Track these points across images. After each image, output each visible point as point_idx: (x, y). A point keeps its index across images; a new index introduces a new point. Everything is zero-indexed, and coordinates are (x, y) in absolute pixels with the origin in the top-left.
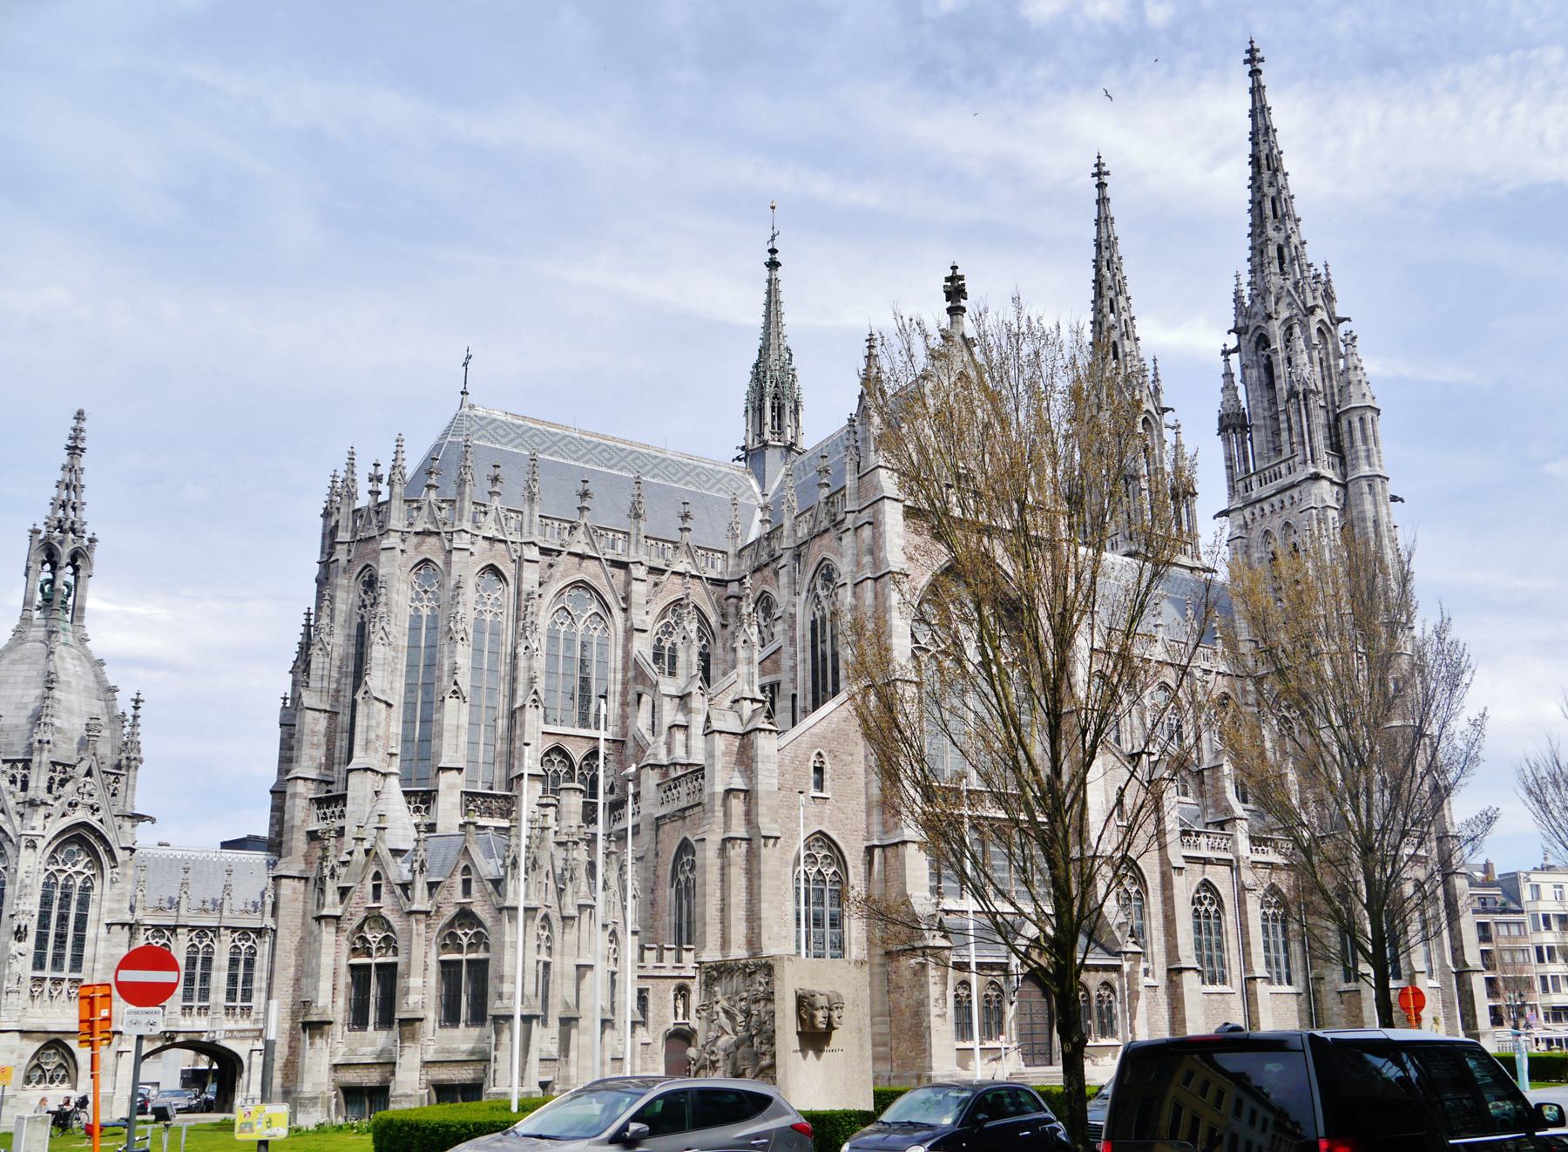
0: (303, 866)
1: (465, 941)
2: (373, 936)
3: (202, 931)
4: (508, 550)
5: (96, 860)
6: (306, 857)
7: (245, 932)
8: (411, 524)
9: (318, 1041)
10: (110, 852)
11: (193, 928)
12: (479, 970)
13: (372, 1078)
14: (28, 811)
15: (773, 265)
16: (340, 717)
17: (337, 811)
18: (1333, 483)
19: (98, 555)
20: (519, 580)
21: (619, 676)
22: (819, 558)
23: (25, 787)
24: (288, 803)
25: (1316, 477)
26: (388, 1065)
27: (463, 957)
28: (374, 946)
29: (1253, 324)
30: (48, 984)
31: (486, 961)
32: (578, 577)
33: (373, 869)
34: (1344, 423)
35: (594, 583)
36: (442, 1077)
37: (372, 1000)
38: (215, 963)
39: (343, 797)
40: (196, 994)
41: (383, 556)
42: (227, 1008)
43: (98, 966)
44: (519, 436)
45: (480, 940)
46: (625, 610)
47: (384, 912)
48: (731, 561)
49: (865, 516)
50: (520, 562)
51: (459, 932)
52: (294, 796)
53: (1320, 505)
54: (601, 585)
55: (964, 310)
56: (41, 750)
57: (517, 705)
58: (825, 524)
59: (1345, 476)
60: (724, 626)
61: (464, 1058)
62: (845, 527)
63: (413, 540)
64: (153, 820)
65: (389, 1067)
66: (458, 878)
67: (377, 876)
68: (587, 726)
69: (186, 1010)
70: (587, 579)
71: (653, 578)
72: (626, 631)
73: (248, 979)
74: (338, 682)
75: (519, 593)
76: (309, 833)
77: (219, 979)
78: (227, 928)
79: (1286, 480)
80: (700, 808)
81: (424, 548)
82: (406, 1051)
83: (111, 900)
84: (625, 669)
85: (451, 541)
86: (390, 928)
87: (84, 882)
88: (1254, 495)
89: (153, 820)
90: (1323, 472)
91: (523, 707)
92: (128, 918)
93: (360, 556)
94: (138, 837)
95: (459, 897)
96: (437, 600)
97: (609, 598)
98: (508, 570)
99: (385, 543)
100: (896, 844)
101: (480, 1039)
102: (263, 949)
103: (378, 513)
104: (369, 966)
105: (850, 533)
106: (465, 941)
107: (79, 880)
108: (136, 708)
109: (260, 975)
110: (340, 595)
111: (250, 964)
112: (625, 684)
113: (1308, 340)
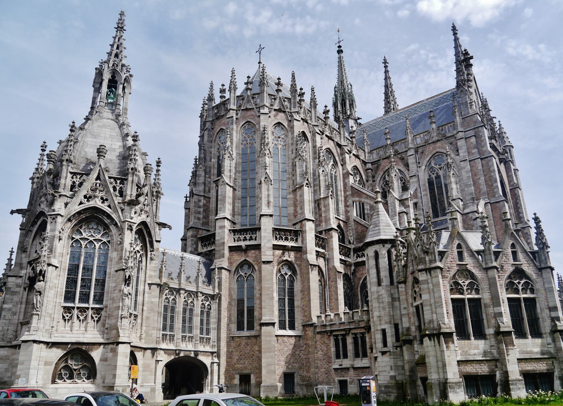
0: (227, 264)
1: (520, 287)
2: (464, 282)
3: (190, 293)
4: (309, 126)
5: (144, 247)
6: (229, 259)
8: (272, 105)
9: (451, 345)
11: (186, 291)
12: (531, 303)
13: (484, 369)
14: (126, 208)
15: (340, 52)
16: (237, 192)
17: (248, 237)
19: (133, 81)
20: (314, 141)
21: (343, 193)
22: (434, 152)
23: (121, 194)
24: (218, 231)
26: (498, 361)
28: (465, 288)
31: (534, 300)
33: (456, 242)
36: (528, 368)
38: (195, 312)
40: (187, 329)
41: (262, 117)
42: (201, 338)
43: (145, 308)
45: (529, 286)
46: (342, 165)
47: (469, 267)
48: (367, 155)
49: (472, 133)
50: (314, 134)
51: (515, 282)
52: (223, 227)
55: (472, 65)
56: (133, 174)
57: (322, 197)
58: (435, 138)
60: (367, 181)
61: (539, 356)
63: (273, 113)
64: (170, 227)
65: (493, 363)
67: (459, 246)
70: (331, 148)
74: (235, 174)
75: (314, 147)
76: (229, 247)
77: (197, 320)
78: (201, 293)
81: (278, 117)
82: (510, 352)
83: (151, 270)
84: (345, 192)
86: (472, 276)
89: (170, 227)
91: (326, 198)
92: (158, 281)
93: (243, 117)
94: (162, 236)
95: (511, 261)
98: (309, 135)
101: (542, 345)
102: (214, 306)
103: (253, 98)
104: (463, 300)
105: (464, 139)
106: (520, 287)
108: (158, 166)
109: (213, 320)
110: (234, 134)
112: (346, 197)
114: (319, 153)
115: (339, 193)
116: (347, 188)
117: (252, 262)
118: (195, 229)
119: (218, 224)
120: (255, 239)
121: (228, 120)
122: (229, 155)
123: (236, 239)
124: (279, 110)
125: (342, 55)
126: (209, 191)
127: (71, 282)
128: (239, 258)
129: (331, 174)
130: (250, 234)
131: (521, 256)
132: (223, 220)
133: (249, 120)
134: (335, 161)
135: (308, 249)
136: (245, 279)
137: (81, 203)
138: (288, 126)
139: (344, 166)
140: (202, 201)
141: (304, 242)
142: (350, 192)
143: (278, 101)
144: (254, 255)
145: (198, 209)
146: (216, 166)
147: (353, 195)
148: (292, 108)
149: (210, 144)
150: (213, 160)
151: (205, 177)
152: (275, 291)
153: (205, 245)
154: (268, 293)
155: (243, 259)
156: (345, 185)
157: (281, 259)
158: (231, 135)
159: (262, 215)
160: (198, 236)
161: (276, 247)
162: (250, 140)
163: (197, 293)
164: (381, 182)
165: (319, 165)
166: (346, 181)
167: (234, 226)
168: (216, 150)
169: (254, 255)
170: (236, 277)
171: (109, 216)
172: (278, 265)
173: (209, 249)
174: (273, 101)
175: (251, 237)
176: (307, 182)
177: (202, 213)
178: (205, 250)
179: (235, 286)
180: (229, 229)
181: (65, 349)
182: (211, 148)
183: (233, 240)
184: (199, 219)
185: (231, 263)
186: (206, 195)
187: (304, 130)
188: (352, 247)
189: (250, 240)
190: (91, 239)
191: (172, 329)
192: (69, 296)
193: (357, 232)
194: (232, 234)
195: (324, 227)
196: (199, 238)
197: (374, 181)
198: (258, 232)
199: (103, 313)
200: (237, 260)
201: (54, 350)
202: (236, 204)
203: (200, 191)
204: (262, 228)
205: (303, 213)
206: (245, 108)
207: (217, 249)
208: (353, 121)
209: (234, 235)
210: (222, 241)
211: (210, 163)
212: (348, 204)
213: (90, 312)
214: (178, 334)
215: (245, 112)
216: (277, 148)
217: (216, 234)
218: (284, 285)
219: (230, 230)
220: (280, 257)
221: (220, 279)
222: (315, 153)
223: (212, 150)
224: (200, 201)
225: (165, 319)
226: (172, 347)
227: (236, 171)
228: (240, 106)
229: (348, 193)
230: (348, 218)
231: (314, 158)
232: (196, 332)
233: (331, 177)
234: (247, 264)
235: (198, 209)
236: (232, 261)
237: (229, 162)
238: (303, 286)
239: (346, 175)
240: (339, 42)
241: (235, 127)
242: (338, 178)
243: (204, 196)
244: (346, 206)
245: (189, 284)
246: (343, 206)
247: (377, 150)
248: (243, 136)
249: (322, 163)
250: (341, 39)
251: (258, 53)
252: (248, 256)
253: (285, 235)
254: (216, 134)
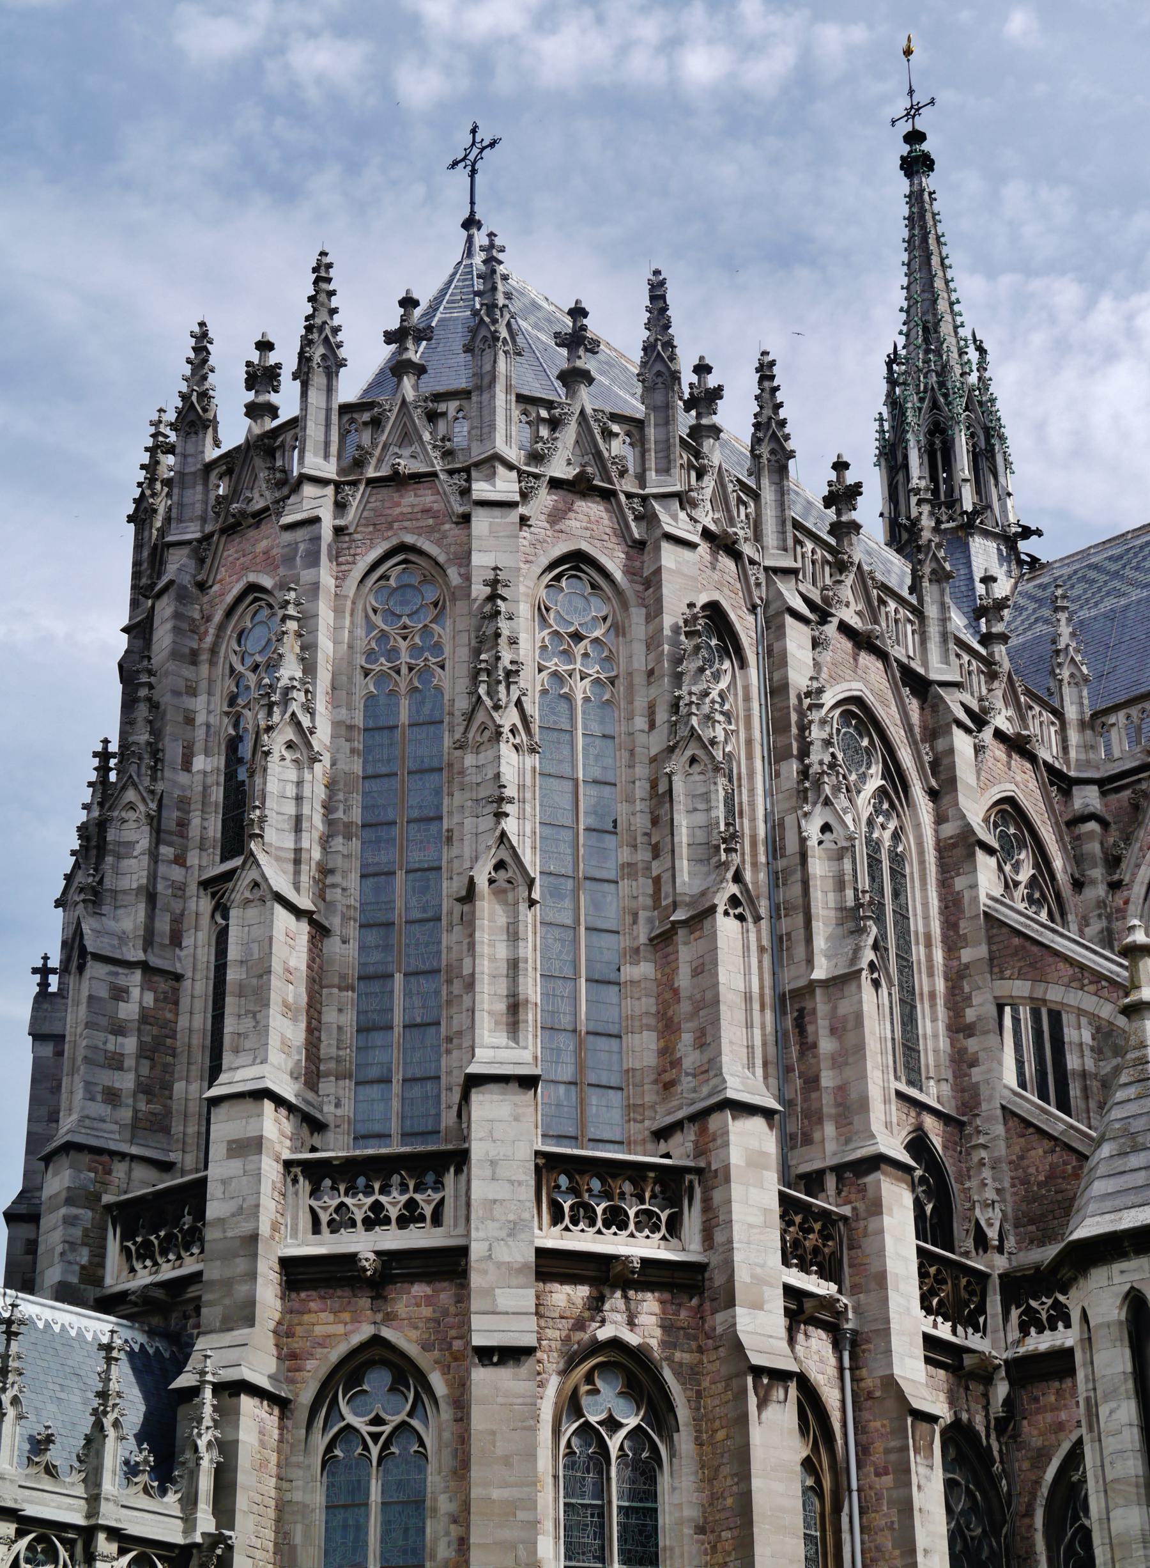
4: (743, 577)
6: (283, 1333)
8: (536, 457)
15: (917, 164)
21: (939, 955)
24: (220, 1169)
41: (481, 522)
46: (933, 794)
48: (1074, 737)
50: (773, 619)
52: (252, 1146)
57: (819, 974)
60: (1078, 885)
63: (545, 499)
70: (870, 699)
72: (942, 848)
74: (325, 842)
75: (777, 690)
76: (287, 1264)
78: (114, 1533)
81: (573, 523)
84: (952, 947)
85: (648, 518)
93: (377, 524)
96: (609, 660)
98: (746, 626)
99: (481, 489)
103: (432, 417)
112: (956, 977)
114: (804, 728)
115: (918, 952)
116: (964, 927)
117: (412, 1349)
118: (86, 1158)
119: (226, 1127)
120: (437, 1220)
121: (288, 536)
122: (290, 734)
123: (324, 1218)
124: (577, 487)
125: (930, 182)
126: (176, 940)
128: (339, 1330)
129: (874, 846)
130: (404, 1188)
132: (249, 1105)
133: (409, 539)
134: (895, 774)
135: (742, 1275)
136: (375, 1451)
138: (629, 571)
139: (946, 801)
140: (135, 993)
141: (719, 1237)
142: (982, 951)
143: (569, 433)
144: (427, 1312)
145: (112, 1043)
146: (218, 794)
147: (995, 964)
148: (652, 475)
149: (188, 672)
150: (200, 763)
151: (154, 856)
152: (549, 1525)
153: (146, 1253)
154: (507, 1534)
155: (365, 1332)
156: (952, 906)
157: (585, 1337)
158: (307, 620)
159: (475, 1081)
160: (107, 1199)
161: (552, 1266)
162: (415, 650)
163: (88, 1533)
165: (803, 795)
166: (959, 883)
167: (316, 1140)
168: (220, 704)
169: (427, 1312)
170: (320, 1442)
172: (565, 1373)
173: (167, 1272)
174: (544, 432)
175: (411, 1204)
176: (734, 889)
177: (129, 1062)
178: (144, 1278)
179: (313, 1495)
180: (287, 1155)
182: (192, 692)
183: (305, 1220)
184: (112, 1096)
185: (294, 1356)
186: (155, 961)
187: (716, 596)
188: (998, 1264)
189: (403, 1222)
193: (1025, 1182)
194: (304, 1185)
195: (830, 1148)
196: (108, 1208)
197: (1115, 886)
198: (449, 1179)
200: (325, 1342)
202: (330, 1016)
203: (122, 938)
204: (478, 1150)
205: (711, 1068)
206: (384, 472)
207: (213, 1273)
208: (992, 545)
209: (315, 1193)
210: (245, 1228)
211: (183, 778)
212: (970, 1015)
215: (384, 493)
216: (568, 698)
217: (213, 1189)
218: (601, 1490)
219: (288, 1164)
220: (580, 1325)
221: (227, 1449)
222: (778, 724)
223: (199, 704)
224: (119, 994)
227: (329, 822)
228: (359, 463)
229: (966, 955)
230: (969, 1098)
231: (777, 756)
233: (874, 863)
234: (385, 1363)
235: (112, 1043)
236: (297, 1344)
237: (292, 775)
238: (714, 1498)
239: (959, 852)
240: (913, 112)
241: (326, 575)
242: (911, 868)
243: (144, 966)
244: (959, 1028)
245: (47, 1483)
246: (941, 1026)
247: (1134, 711)
248: (370, 626)
249: (818, 785)
250: (920, 97)
251: (462, 173)
252: (389, 1318)
253: (607, 1195)
254: (218, 617)
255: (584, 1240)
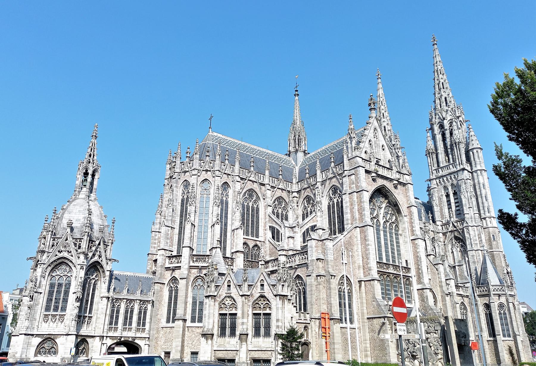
7: (144, 301)
10: (104, 272)
17: (176, 261)
18: (469, 172)
22: (331, 185)
25: (464, 169)
27: (261, 312)
29: (437, 121)
30: (82, 318)
32: (251, 187)
34: (471, 153)
35: (255, 190)
37: (227, 327)
39: (181, 256)
44: (227, 143)
47: (232, 295)
53: (465, 178)
54: (257, 190)
59: (472, 169)
62: (344, 175)
66: (259, 284)
68: (253, 236)
69: (124, 329)
70: (253, 188)
71: (272, 189)
73: (145, 319)
79: (453, 170)
80: (305, 265)
87: (95, 282)
88: (440, 175)
90: (466, 168)
97: (260, 195)
100: (370, 280)
107: (93, 281)
111: (145, 313)
113: (458, 126)
127: (49, 300)
131: (266, 287)
134: (258, 197)
137: (56, 255)
164: (302, 207)
167: (172, 253)
170: (168, 288)
171: (71, 262)
174: (202, 164)
181: (42, 338)
190: (62, 275)
191: (116, 323)
192: (48, 309)
199: (65, 317)
201: (37, 338)
213: (58, 317)
214: (134, 324)
225: (112, 317)
226: (116, 334)
232: (134, 324)
255: (196, 264)
